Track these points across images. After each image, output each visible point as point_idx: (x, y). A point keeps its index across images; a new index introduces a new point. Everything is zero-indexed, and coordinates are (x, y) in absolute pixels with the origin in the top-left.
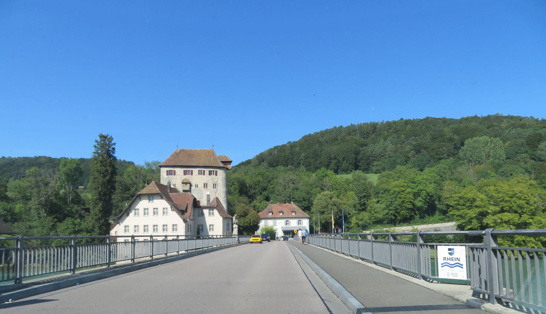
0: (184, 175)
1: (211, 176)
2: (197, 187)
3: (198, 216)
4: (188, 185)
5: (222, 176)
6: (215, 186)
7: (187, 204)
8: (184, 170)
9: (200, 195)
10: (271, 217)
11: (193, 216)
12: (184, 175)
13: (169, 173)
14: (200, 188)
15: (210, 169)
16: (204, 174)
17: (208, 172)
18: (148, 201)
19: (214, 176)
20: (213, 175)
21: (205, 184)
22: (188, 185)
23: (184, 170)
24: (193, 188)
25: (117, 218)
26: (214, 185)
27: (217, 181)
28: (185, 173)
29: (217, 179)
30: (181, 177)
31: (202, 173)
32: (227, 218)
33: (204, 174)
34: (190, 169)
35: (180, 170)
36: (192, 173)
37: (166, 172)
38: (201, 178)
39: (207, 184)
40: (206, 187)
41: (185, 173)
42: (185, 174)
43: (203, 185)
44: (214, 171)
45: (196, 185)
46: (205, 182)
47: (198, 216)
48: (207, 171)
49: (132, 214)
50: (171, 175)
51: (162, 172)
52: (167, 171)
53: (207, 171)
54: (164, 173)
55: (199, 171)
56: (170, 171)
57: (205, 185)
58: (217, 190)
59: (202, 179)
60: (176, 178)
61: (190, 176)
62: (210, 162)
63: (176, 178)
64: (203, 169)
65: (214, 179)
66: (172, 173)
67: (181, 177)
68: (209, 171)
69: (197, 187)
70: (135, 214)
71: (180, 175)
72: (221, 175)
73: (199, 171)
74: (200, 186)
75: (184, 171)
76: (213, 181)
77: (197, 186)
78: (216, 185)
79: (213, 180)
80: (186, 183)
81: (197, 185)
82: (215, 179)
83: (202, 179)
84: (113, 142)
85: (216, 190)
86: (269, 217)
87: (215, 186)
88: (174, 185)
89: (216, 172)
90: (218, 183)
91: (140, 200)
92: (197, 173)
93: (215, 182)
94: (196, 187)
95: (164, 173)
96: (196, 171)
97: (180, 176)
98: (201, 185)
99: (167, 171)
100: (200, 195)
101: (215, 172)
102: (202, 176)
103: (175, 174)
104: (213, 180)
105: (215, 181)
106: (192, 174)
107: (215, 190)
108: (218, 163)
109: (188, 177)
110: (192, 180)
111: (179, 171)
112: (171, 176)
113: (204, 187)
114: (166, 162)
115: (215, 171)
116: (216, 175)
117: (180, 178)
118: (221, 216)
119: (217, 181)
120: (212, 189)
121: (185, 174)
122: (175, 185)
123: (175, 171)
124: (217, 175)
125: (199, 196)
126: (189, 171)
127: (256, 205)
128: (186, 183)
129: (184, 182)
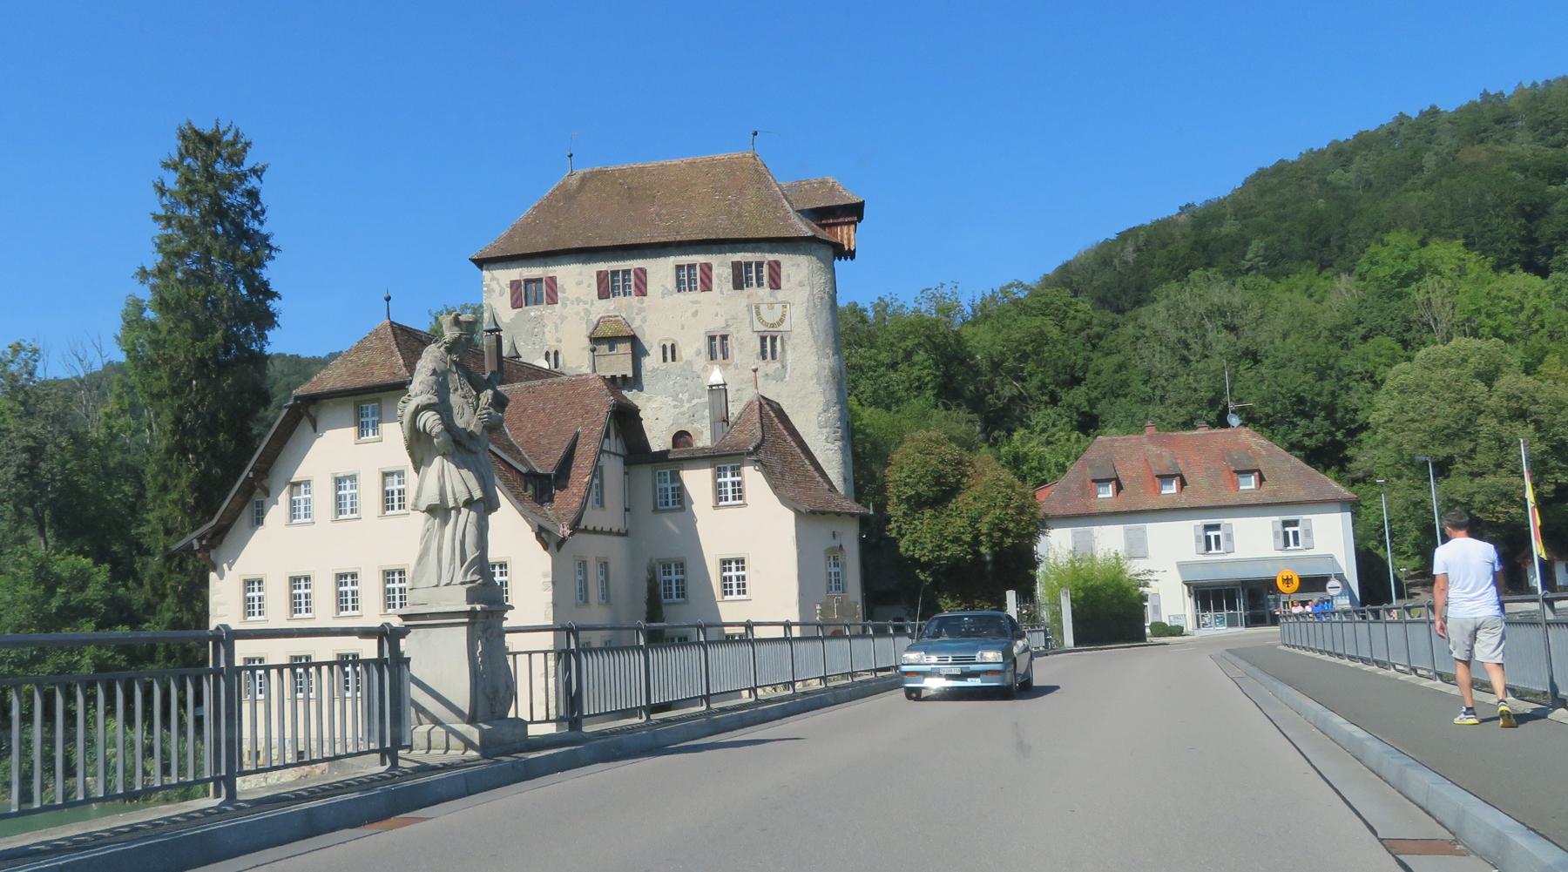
0: (601, 296)
1: (747, 291)
2: (674, 359)
3: (656, 510)
4: (624, 348)
5: (808, 289)
6: (769, 345)
7: (570, 437)
8: (599, 273)
9: (689, 401)
10: (1109, 509)
11: (627, 510)
12: (601, 296)
13: (523, 295)
14: (690, 363)
15: (740, 257)
16: (707, 286)
17: (727, 272)
18: (352, 431)
19: (765, 291)
20: (760, 284)
21: (712, 338)
22: (624, 348)
23: (599, 273)
24: (651, 362)
25: (200, 539)
26: (763, 339)
27: (782, 320)
28: (607, 287)
29: (778, 308)
30: (587, 312)
32: (823, 513)
33: (707, 286)
35: (580, 274)
36: (645, 285)
37: (508, 291)
38: (695, 307)
39: (724, 338)
40: (720, 356)
41: (607, 287)
42: (603, 294)
43: (703, 344)
44: (759, 265)
45: (664, 347)
46: (717, 326)
47: (656, 510)
48: (721, 265)
49: (277, 513)
50: (537, 302)
51: (491, 291)
52: (514, 285)
53: (721, 265)
54: (502, 294)
55: (679, 268)
56: (528, 281)
57: (718, 346)
58: (784, 367)
59: (695, 314)
60: (562, 318)
61: (634, 299)
62: (739, 216)
63: (562, 318)
64: (698, 259)
65: (763, 308)
66: (537, 290)
67: (587, 312)
68: (736, 266)
69: (674, 359)
70: (293, 513)
71: (579, 300)
72: (801, 284)
73: (679, 268)
74: (685, 352)
76: (760, 319)
78: (774, 339)
79: (758, 313)
80: (612, 341)
81: (673, 346)
82: (771, 306)
83: (695, 314)
84: (248, 164)
85: (778, 365)
86: (1101, 508)
87: (769, 345)
88: (552, 357)
89: (775, 268)
90: (785, 327)
91: (315, 431)
92: (671, 283)
93: (773, 325)
94: (665, 360)
95: (502, 294)
96: (660, 270)
97: (582, 306)
98: (692, 348)
99: (514, 285)
100: (689, 401)
101: (765, 269)
102: (697, 295)
103: (553, 300)
104: (758, 313)
105: (770, 316)
106: (642, 291)
107: (772, 367)
108: (786, 218)
109: (619, 306)
110: (644, 320)
111: (576, 279)
112: (533, 311)
113: (713, 357)
114: (510, 237)
115: (769, 264)
116: (775, 284)
117: (582, 314)
118: (785, 501)
119: (782, 320)
121: (603, 294)
122: (556, 353)
123: (552, 280)
124: (778, 287)
125: (687, 405)
126: (626, 272)
127: (1026, 454)
128: (612, 341)
129: (600, 334)
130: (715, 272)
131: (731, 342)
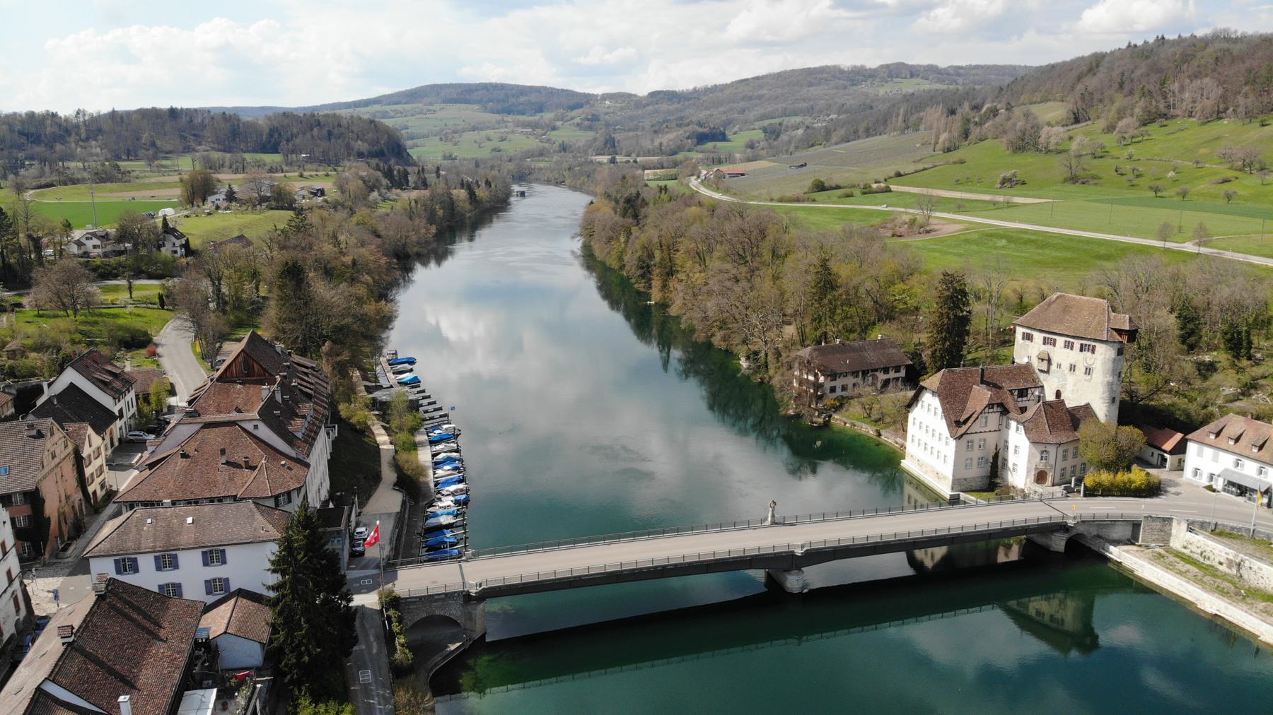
1: (1084, 353)
4: (1046, 362)
6: (1088, 371)
15: (1084, 342)
17: (1079, 346)
19: (1089, 354)
24: (1054, 367)
28: (1045, 341)
31: (1069, 346)
34: (1054, 337)
41: (1045, 341)
42: (1044, 344)
43: (1068, 366)
46: (1073, 362)
48: (1077, 343)
64: (1071, 340)
68: (1082, 345)
74: (1063, 366)
75: (1045, 339)
77: (1059, 366)
87: (1088, 371)
89: (1094, 347)
92: (1063, 345)
96: (1060, 341)
98: (1066, 366)
102: (1069, 350)
107: (1089, 377)
109: (1048, 348)
111: (1038, 337)
116: (1093, 352)
120: (1083, 375)
121: (1044, 344)
130: (1075, 345)
131: (1076, 368)
